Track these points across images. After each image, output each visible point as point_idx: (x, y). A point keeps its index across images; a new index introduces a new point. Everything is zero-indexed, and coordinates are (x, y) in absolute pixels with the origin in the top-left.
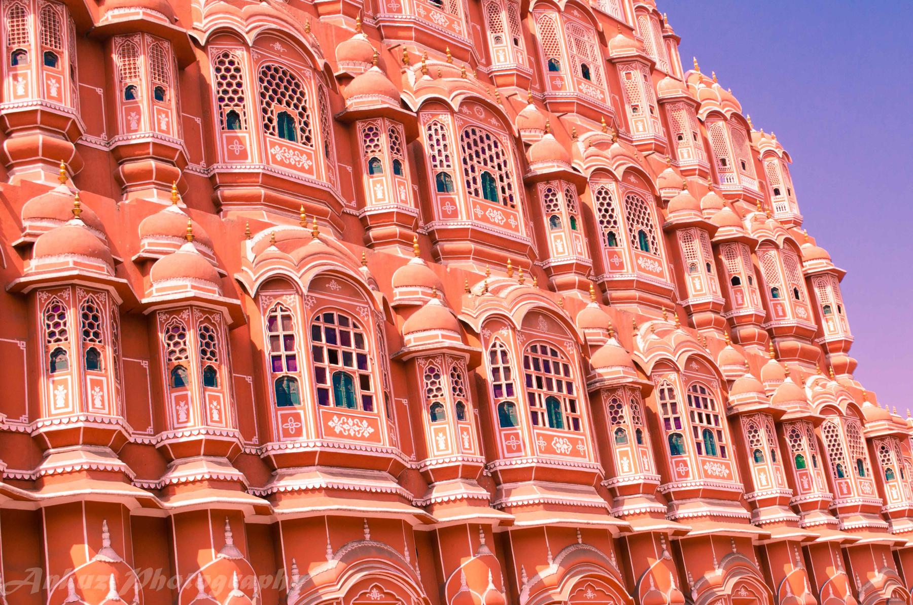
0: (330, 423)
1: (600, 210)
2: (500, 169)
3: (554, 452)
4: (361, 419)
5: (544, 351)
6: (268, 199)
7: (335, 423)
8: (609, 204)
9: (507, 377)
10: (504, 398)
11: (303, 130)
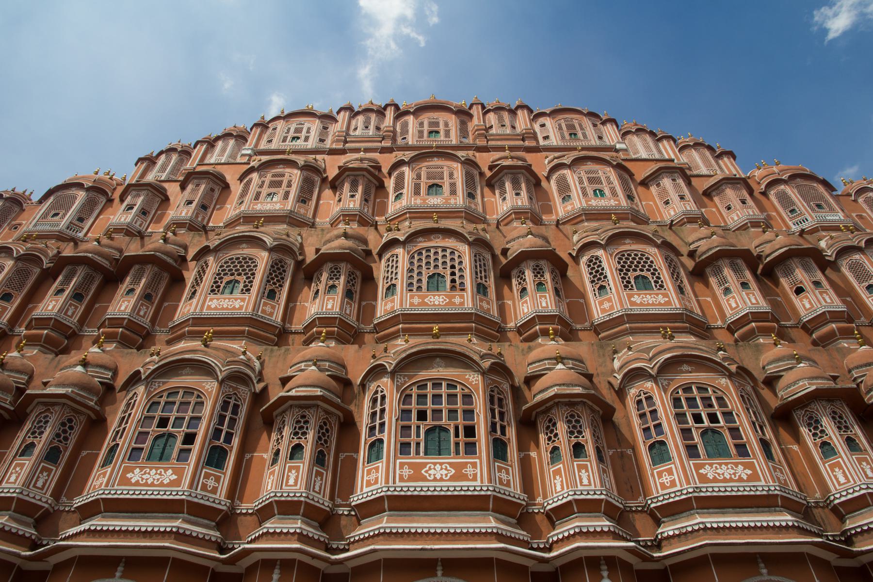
0: (129, 475)
1: (591, 273)
2: (453, 267)
3: (425, 479)
4: (166, 469)
5: (437, 385)
6: (189, 332)
7: (135, 476)
8: (599, 266)
9: (381, 418)
10: (378, 436)
11: (245, 286)
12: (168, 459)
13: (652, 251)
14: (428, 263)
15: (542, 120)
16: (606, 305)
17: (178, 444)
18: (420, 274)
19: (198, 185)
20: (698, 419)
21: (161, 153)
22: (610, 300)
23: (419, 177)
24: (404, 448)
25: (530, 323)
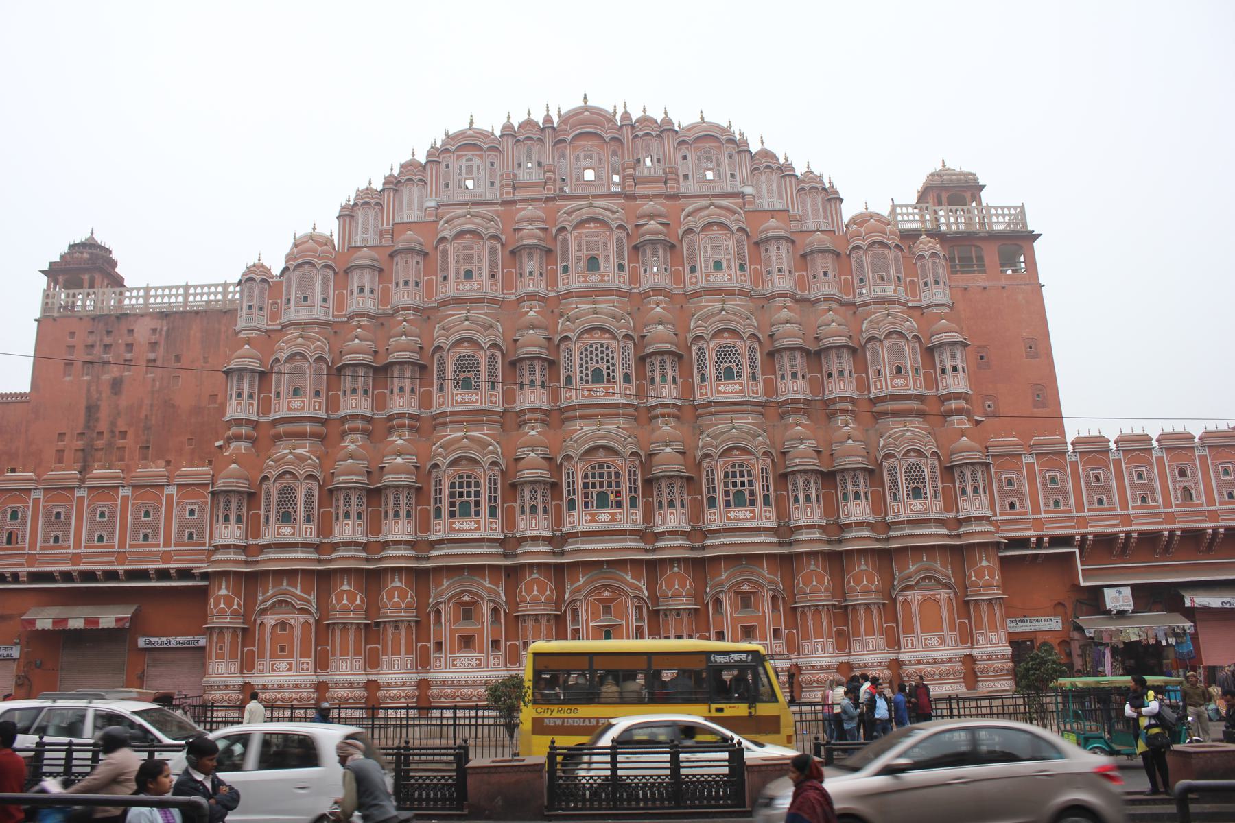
5: (601, 467)
7: (457, 526)
12: (470, 515)
13: (740, 343)
14: (592, 359)
15: (684, 150)
16: (703, 391)
17: (473, 508)
18: (587, 369)
19: (407, 262)
20: (734, 484)
21: (355, 204)
22: (706, 387)
23: (580, 249)
24: (586, 505)
25: (655, 407)
